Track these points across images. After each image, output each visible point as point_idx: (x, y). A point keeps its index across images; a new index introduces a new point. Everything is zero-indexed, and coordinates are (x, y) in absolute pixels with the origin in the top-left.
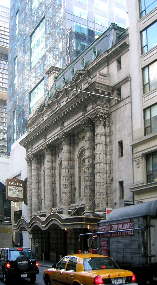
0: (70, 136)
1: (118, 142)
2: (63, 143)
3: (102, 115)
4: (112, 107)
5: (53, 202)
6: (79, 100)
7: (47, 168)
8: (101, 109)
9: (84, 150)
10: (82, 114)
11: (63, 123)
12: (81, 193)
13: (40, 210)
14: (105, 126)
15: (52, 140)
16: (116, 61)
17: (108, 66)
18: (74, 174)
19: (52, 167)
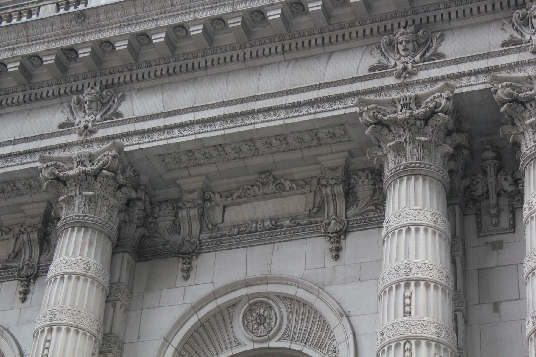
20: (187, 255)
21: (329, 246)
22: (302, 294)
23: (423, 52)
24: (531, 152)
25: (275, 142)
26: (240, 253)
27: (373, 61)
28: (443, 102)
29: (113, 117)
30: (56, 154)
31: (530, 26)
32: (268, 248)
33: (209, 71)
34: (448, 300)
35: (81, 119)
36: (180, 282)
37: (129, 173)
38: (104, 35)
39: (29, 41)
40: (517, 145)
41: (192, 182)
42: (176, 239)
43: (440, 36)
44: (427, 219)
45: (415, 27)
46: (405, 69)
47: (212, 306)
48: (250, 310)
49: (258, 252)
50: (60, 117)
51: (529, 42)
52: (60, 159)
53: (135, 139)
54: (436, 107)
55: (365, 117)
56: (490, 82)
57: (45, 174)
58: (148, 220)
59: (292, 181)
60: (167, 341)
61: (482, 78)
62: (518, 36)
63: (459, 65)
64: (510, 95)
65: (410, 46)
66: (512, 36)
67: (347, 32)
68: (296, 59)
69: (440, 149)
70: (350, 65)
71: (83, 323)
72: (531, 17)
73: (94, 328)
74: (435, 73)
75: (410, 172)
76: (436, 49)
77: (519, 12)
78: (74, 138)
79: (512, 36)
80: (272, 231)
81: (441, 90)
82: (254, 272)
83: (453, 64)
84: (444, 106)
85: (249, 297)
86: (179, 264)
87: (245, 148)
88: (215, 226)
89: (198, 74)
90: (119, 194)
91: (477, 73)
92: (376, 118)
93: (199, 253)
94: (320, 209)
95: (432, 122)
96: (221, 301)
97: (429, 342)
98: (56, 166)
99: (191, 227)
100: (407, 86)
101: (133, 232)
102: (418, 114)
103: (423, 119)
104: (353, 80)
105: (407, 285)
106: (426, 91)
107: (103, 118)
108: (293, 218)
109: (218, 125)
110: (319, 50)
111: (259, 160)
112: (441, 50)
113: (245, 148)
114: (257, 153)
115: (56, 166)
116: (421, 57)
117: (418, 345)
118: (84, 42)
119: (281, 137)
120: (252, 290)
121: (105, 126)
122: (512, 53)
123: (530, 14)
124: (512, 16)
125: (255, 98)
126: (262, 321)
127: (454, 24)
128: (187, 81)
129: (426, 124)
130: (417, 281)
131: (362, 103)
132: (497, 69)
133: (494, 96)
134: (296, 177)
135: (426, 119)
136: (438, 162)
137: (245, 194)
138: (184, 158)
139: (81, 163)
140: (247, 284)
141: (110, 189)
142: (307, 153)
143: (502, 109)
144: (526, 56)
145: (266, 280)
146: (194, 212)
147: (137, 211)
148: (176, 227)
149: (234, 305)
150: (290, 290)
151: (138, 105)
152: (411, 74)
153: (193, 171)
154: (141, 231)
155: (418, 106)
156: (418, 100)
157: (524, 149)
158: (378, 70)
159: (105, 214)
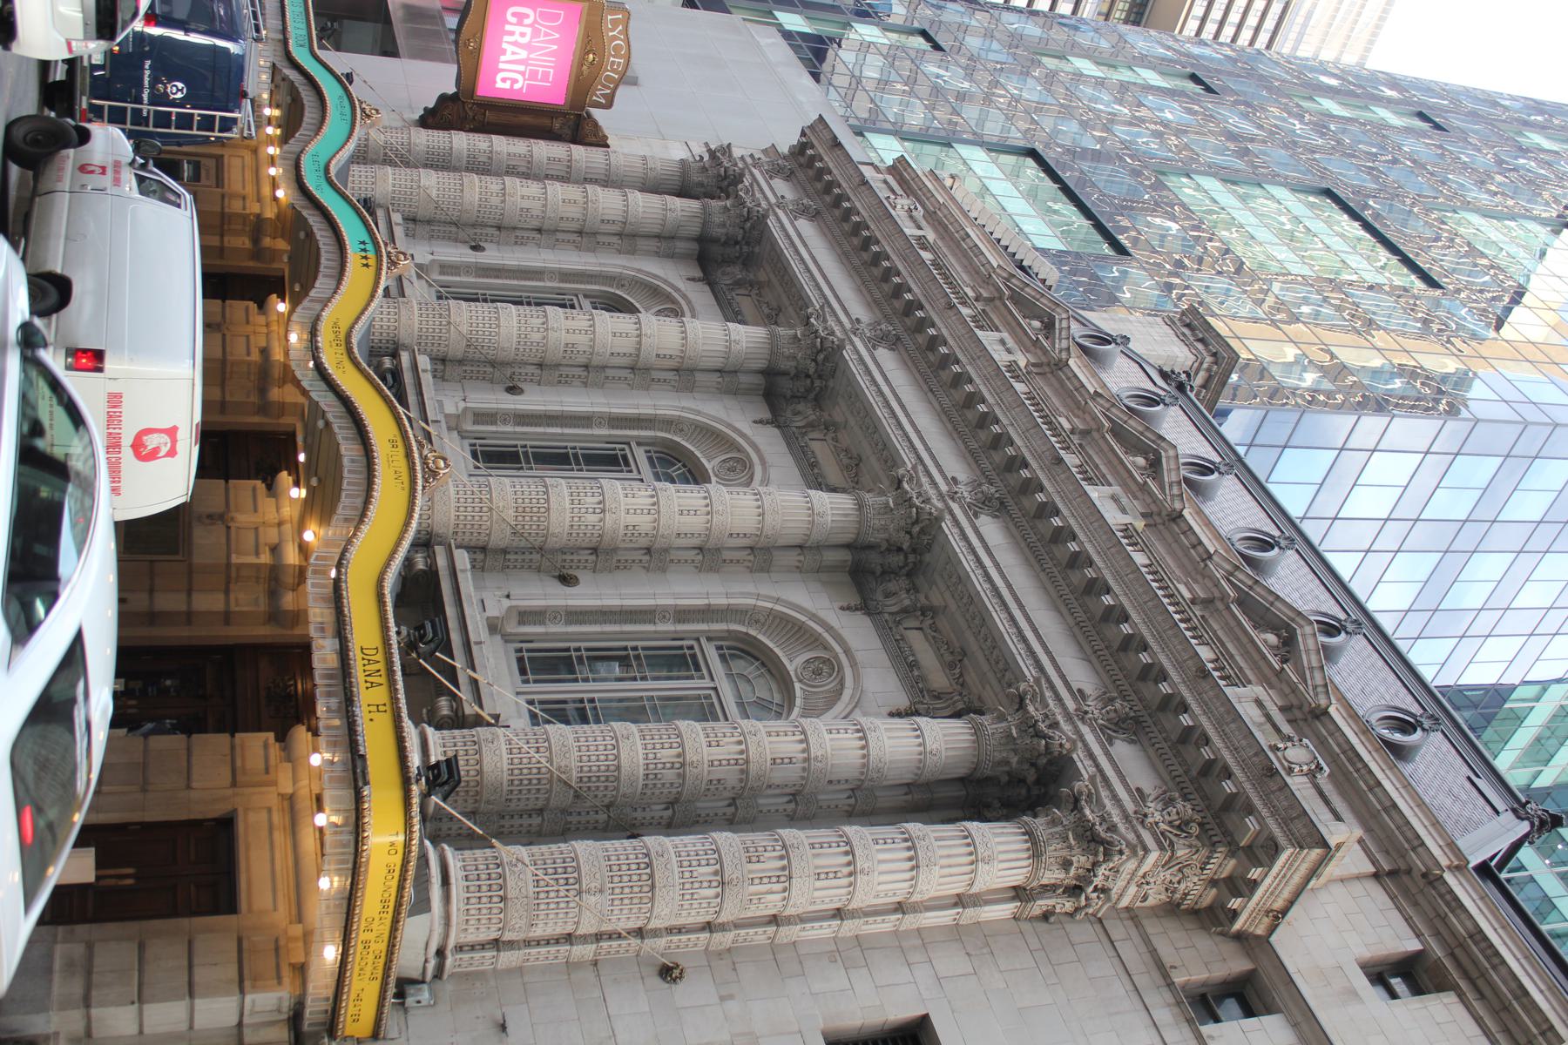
0: (820, 377)
1: (924, 1022)
2: (870, 498)
3: (1101, 877)
4: (1138, 924)
5: (461, 362)
6: (1248, 786)
7: (690, 336)
8: (1138, 877)
9: (676, 313)
10: (858, 320)
11: (894, 343)
12: (542, 623)
13: (411, 226)
14: (1019, 893)
15: (863, 381)
16: (1420, 947)
17: (1376, 876)
18: (663, 570)
19: (692, 371)
20: (866, 606)
21: (902, 708)
22: (847, 693)
25: (989, 643)
26: (877, 643)
27: (1089, 689)
29: (973, 511)
30: (924, 480)
32: (888, 664)
33: (1042, 575)
34: (856, 774)
35: (964, 490)
36: (837, 605)
37: (925, 539)
38: (1046, 483)
39: (1024, 434)
41: (936, 596)
42: (879, 596)
44: (931, 745)
46: (1086, 712)
47: (819, 629)
48: (826, 661)
49: (883, 658)
50: (962, 476)
52: (918, 479)
53: (955, 530)
55: (1022, 686)
57: (901, 471)
58: (888, 573)
59: (961, 675)
60: (778, 600)
61: (1092, 770)
64: (1080, 793)
65: (1112, 715)
67: (1115, 666)
68: (1074, 636)
69: (1012, 754)
70: (1081, 675)
71: (769, 518)
73: (768, 531)
74: (1090, 738)
75: (977, 731)
78: (944, 488)
80: (907, 666)
81: (1069, 739)
82: (859, 656)
85: (836, 656)
86: (855, 600)
87: (977, 621)
88: (899, 623)
89: (1037, 566)
90: (902, 534)
91: (1097, 766)
92: (1025, 693)
93: (869, 614)
94: (938, 697)
95: (1035, 740)
96: (826, 635)
97: (806, 750)
98: (911, 478)
99: (892, 605)
100: (1068, 717)
101: (874, 559)
104: (1063, 677)
105: (858, 731)
107: (969, 505)
108: (922, 678)
109: (986, 586)
110: (1089, 651)
111: (972, 639)
113: (977, 621)
114: (976, 635)
115: (911, 478)
117: (801, 741)
118: (1037, 470)
119: (993, 642)
120: (843, 657)
121: (962, 507)
125: (1021, 607)
126: (817, 673)
127: (1151, 751)
128: (1027, 559)
130: (864, 738)
131: (1037, 681)
132: (1105, 779)
134: (967, 678)
135: (1039, 735)
136: (998, 756)
137: (938, 642)
138: (954, 580)
139: (919, 495)
140: (847, 651)
141: (903, 523)
142: (990, 675)
144: (1130, 807)
145: (854, 664)
146: (907, 602)
147: (896, 560)
148: (888, 595)
149: (826, 647)
150: (849, 682)
151: (991, 528)
152: (1082, 719)
153: (947, 595)
154: (879, 570)
155: (1050, 727)
156: (1055, 725)
158: (1080, 695)
159: (882, 527)
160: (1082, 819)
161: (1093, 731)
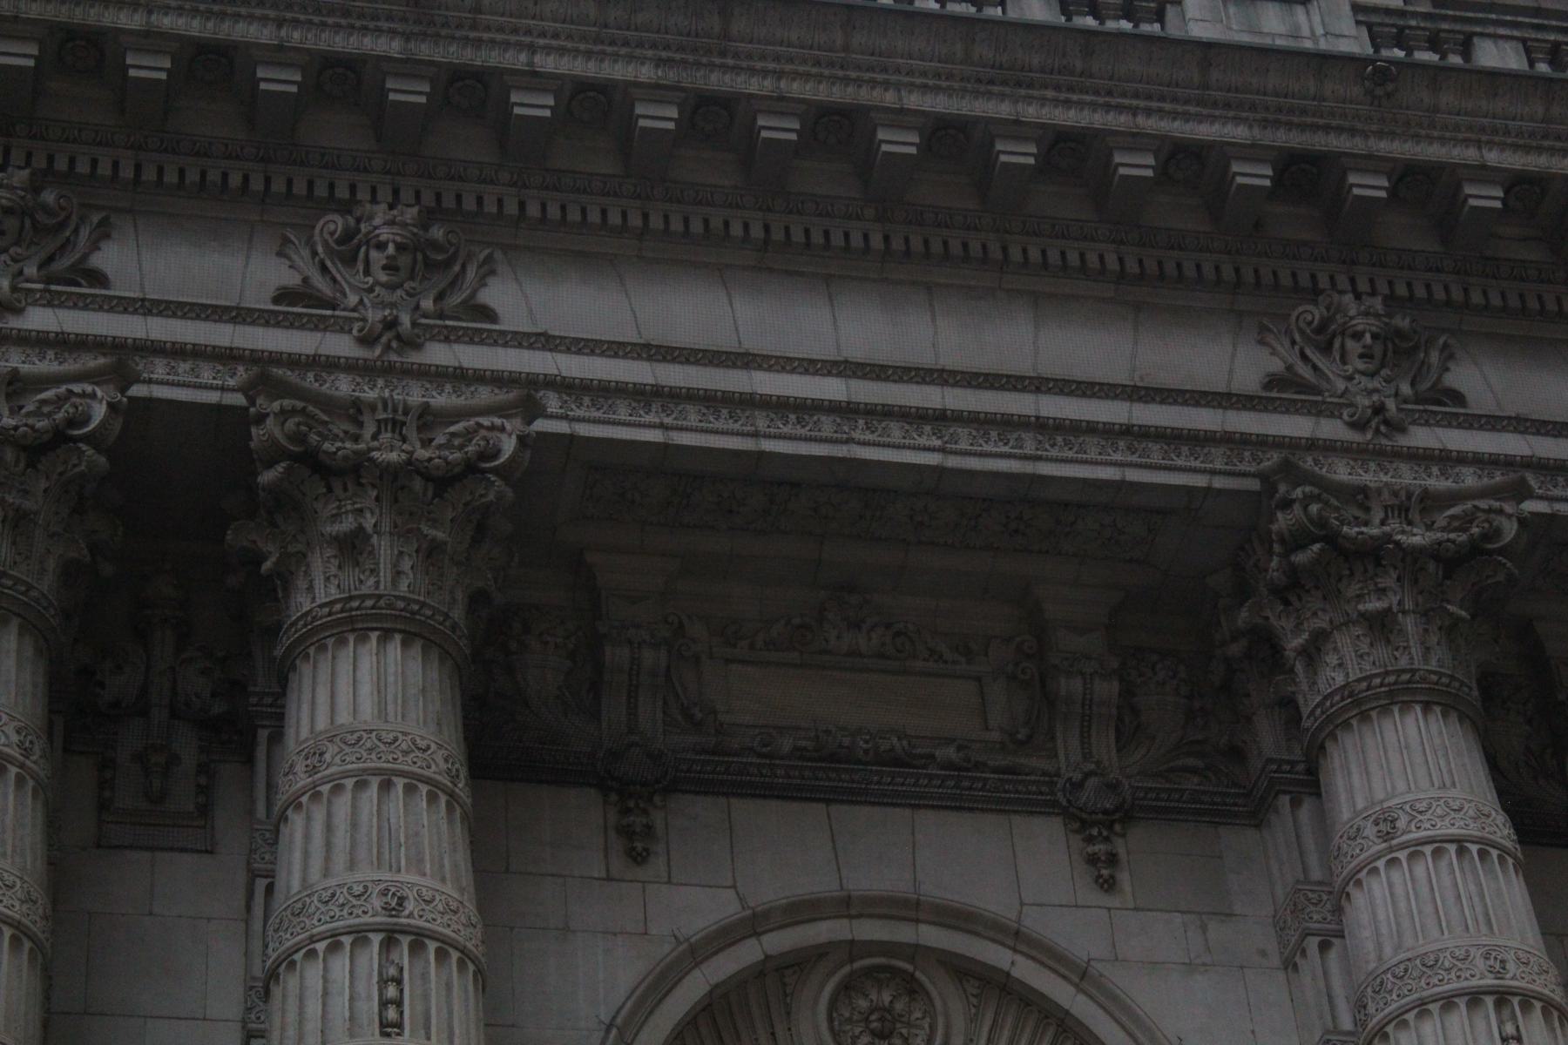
23: (43, 255)
24: (330, 614)
28: (99, 412)
31: (361, 268)
40: (274, 588)
43: (100, 224)
45: (32, 174)
51: (354, 310)
54: (72, 423)
56: (247, 389)
62: (321, 284)
63: (149, 319)
66: (306, 280)
72: (368, 242)
76: (85, 257)
77: (336, 223)
79: (306, 280)
83: (135, 312)
84: (103, 423)
102: (16, 428)
103: (24, 448)
106: (46, 365)
112: (98, 261)
116: (40, 267)
122: (302, 327)
123: (369, 233)
124: (313, 227)
129: (31, 464)
133: (254, 430)
143: (267, 477)
157: (302, 603)
160: (394, 479)
161: (52, 301)
